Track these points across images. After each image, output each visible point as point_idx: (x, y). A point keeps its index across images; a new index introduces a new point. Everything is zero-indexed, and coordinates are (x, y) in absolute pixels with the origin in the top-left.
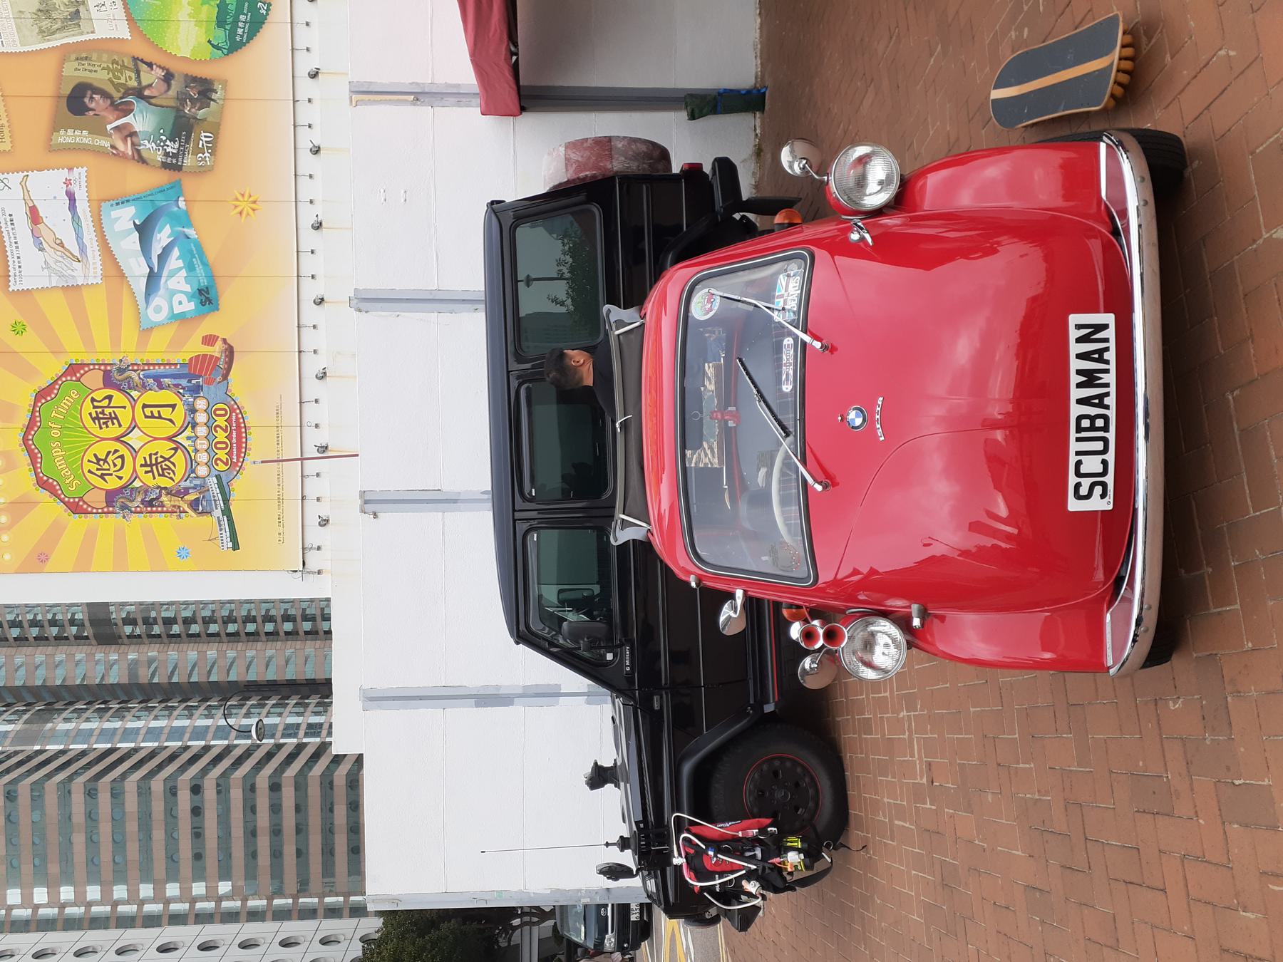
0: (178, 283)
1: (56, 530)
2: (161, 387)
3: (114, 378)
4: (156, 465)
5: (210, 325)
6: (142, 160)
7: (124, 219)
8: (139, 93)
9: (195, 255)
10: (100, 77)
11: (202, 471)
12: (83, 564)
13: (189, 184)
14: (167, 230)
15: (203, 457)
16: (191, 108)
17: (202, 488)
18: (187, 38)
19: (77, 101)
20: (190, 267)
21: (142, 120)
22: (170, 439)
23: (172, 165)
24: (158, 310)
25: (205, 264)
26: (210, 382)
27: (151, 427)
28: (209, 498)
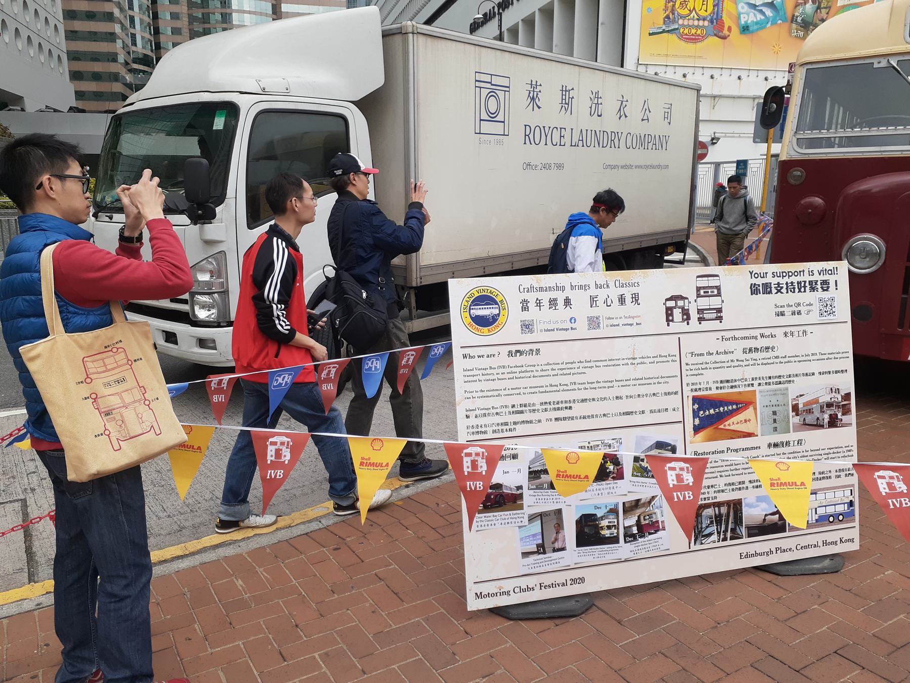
0: (750, 17)
2: (714, 6)
5: (735, 29)
6: (796, 6)
8: (819, 8)
9: (761, 25)
11: (681, 22)
13: (786, 25)
14: (771, 15)
15: (686, 23)
17: (674, 22)
20: (757, 23)
22: (694, 8)
23: (793, 19)
24: (743, 8)
25: (757, 30)
26: (714, 28)
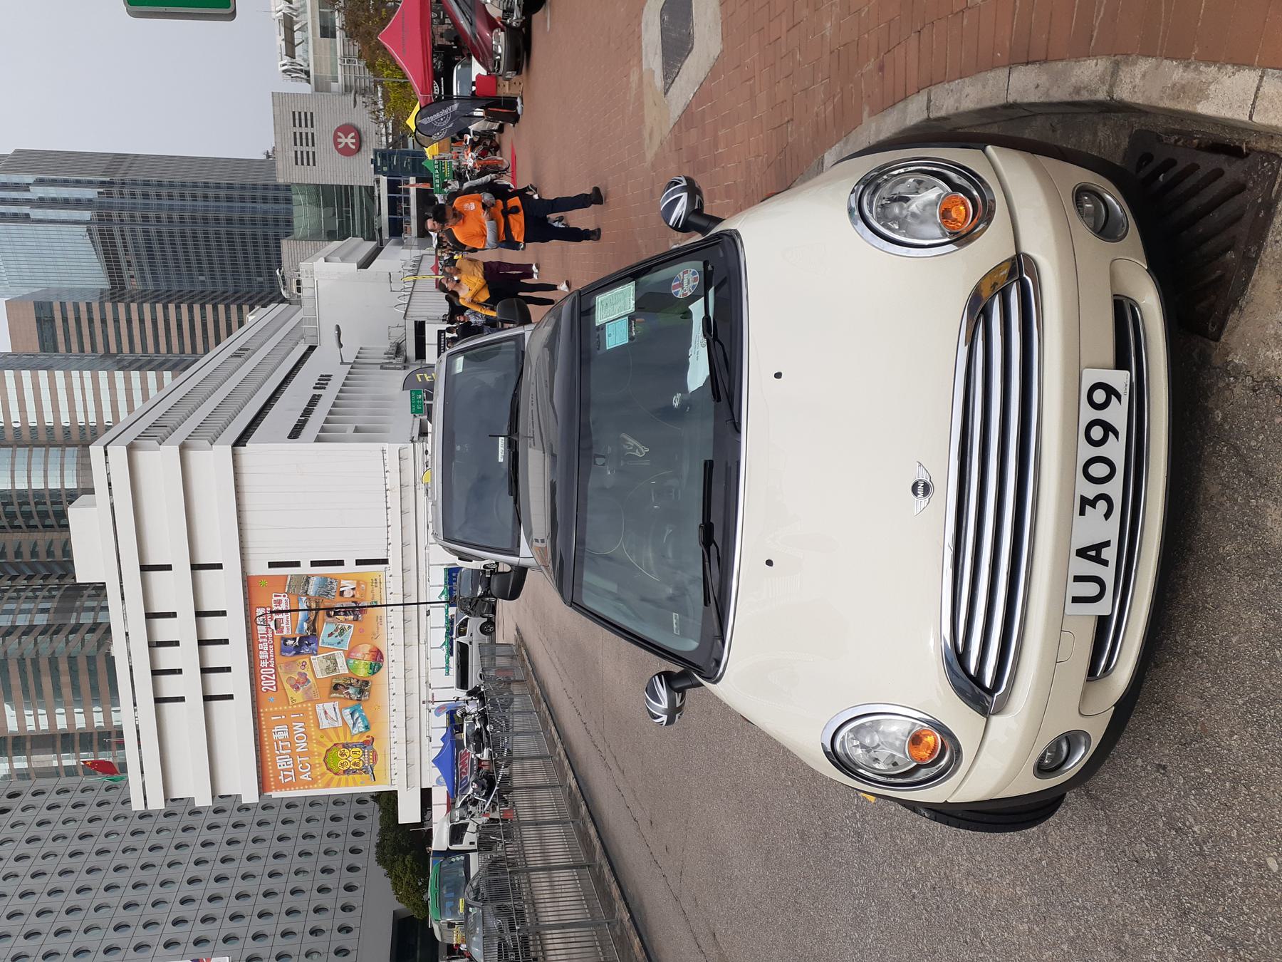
0: (360, 725)
1: (332, 779)
3: (345, 746)
4: (355, 764)
7: (348, 711)
9: (364, 719)
10: (341, 682)
12: (338, 785)
16: (363, 687)
18: (362, 672)
19: (335, 687)
21: (351, 691)
23: (359, 700)
24: (356, 731)
27: (354, 756)
28: (368, 770)
